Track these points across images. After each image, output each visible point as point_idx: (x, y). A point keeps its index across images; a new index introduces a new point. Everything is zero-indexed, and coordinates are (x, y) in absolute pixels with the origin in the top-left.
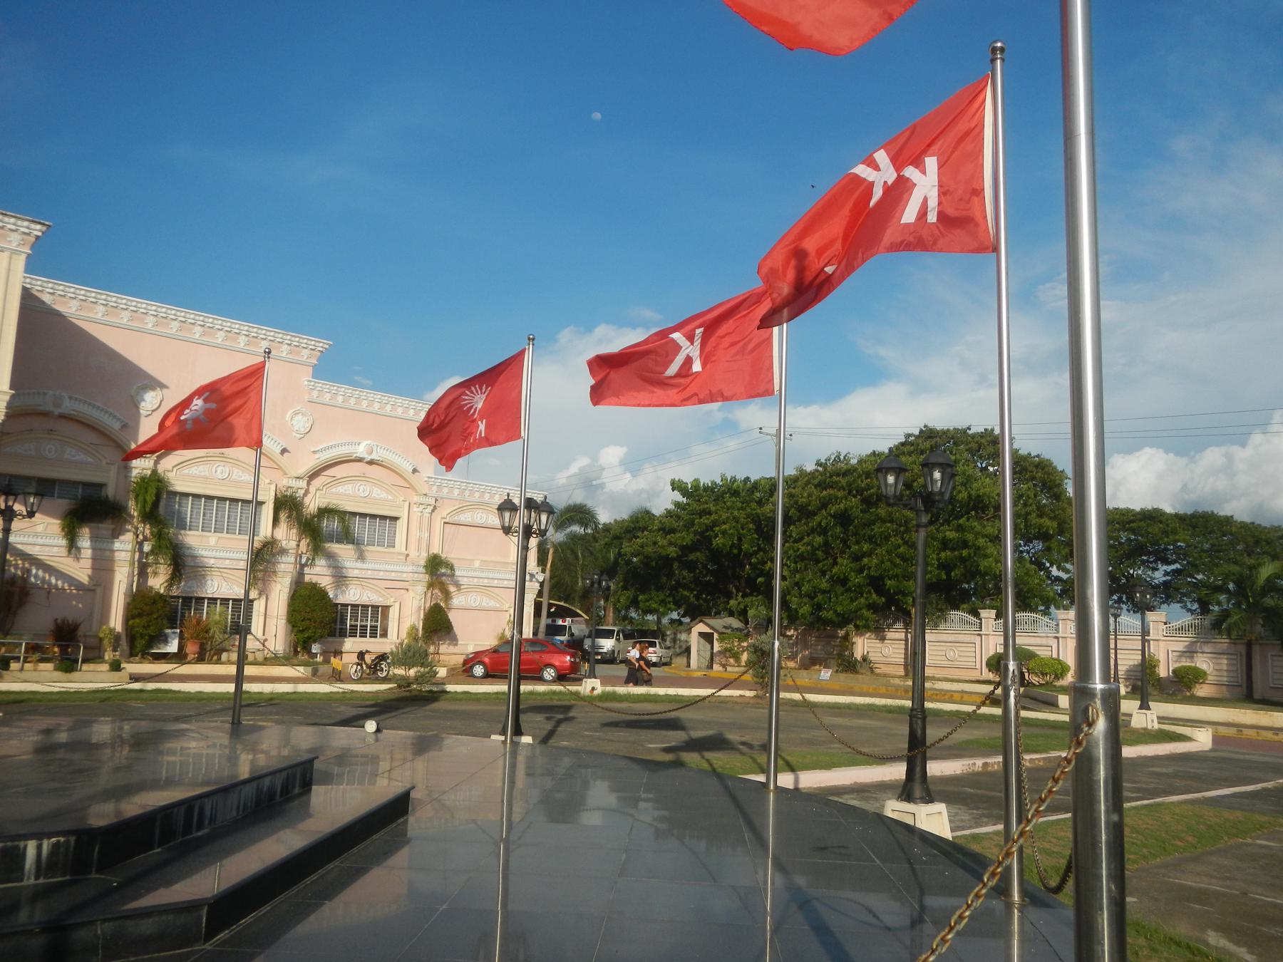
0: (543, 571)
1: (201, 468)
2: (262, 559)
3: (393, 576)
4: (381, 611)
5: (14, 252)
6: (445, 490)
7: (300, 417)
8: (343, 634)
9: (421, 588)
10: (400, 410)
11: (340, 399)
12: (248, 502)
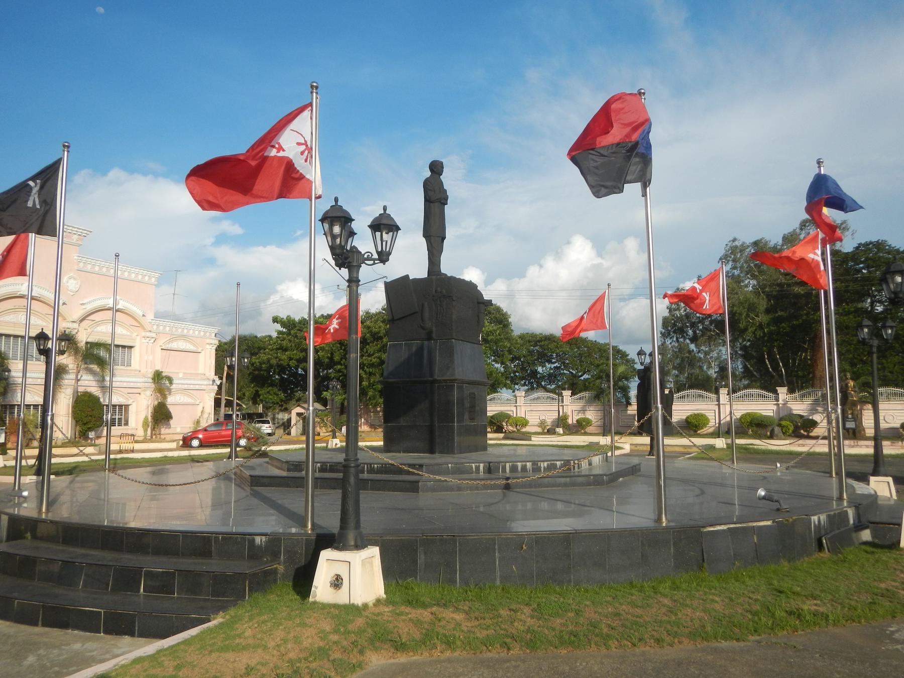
0: (221, 378)
1: (11, 316)
3: (132, 385)
4: (123, 408)
6: (161, 328)
7: (72, 281)
9: (149, 393)
10: (133, 276)
11: (97, 268)
12: (23, 337)
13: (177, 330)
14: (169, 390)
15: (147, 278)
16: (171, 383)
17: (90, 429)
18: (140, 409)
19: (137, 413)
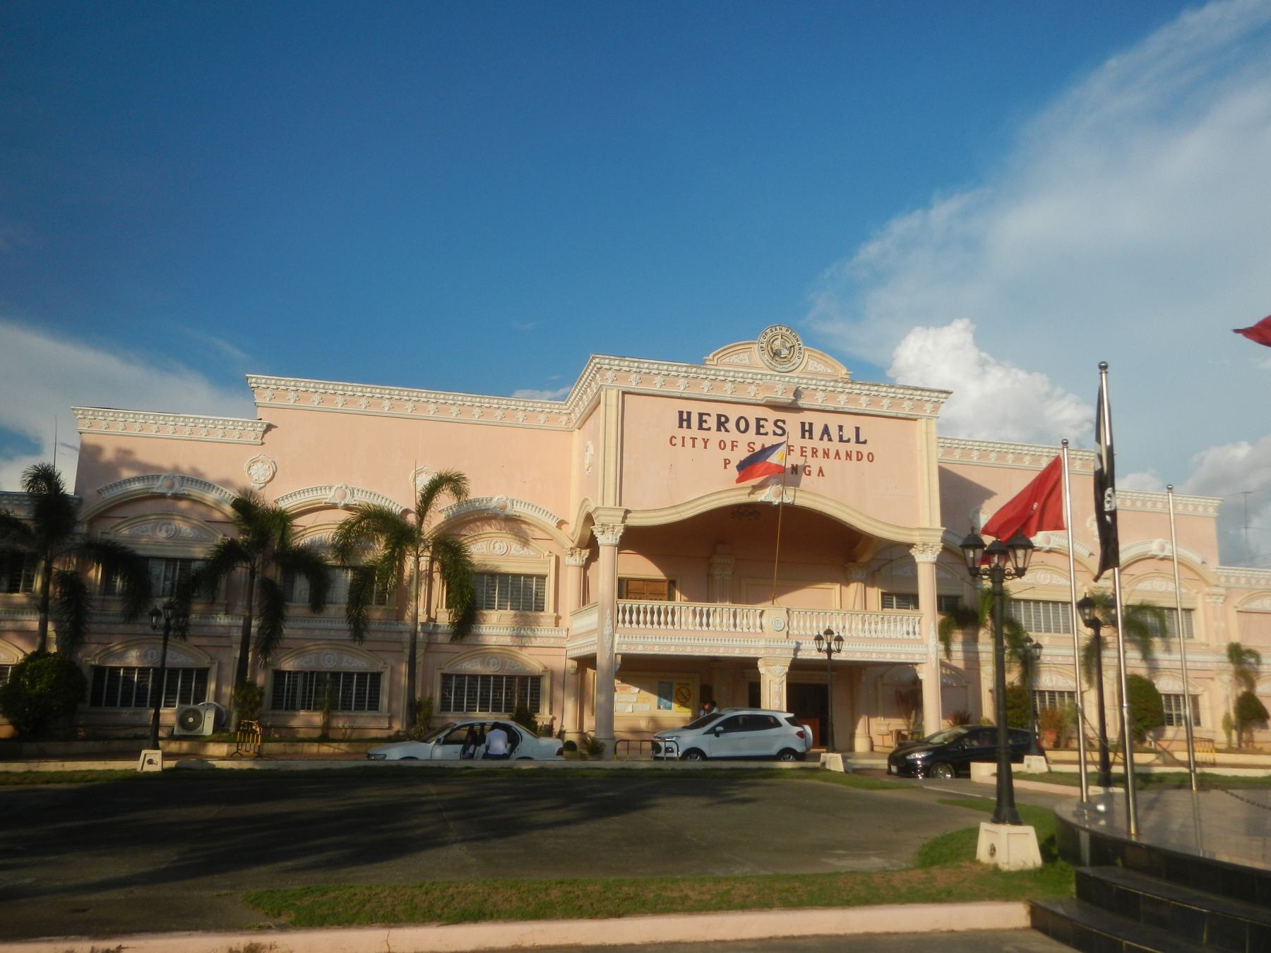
2: (1093, 655)
5: (929, 418)
6: (1233, 580)
8: (1163, 724)
13: (1258, 582)
14: (1258, 673)
15: (1201, 509)
16: (1259, 662)
17: (1148, 728)
18: (1217, 702)
19: (1212, 708)
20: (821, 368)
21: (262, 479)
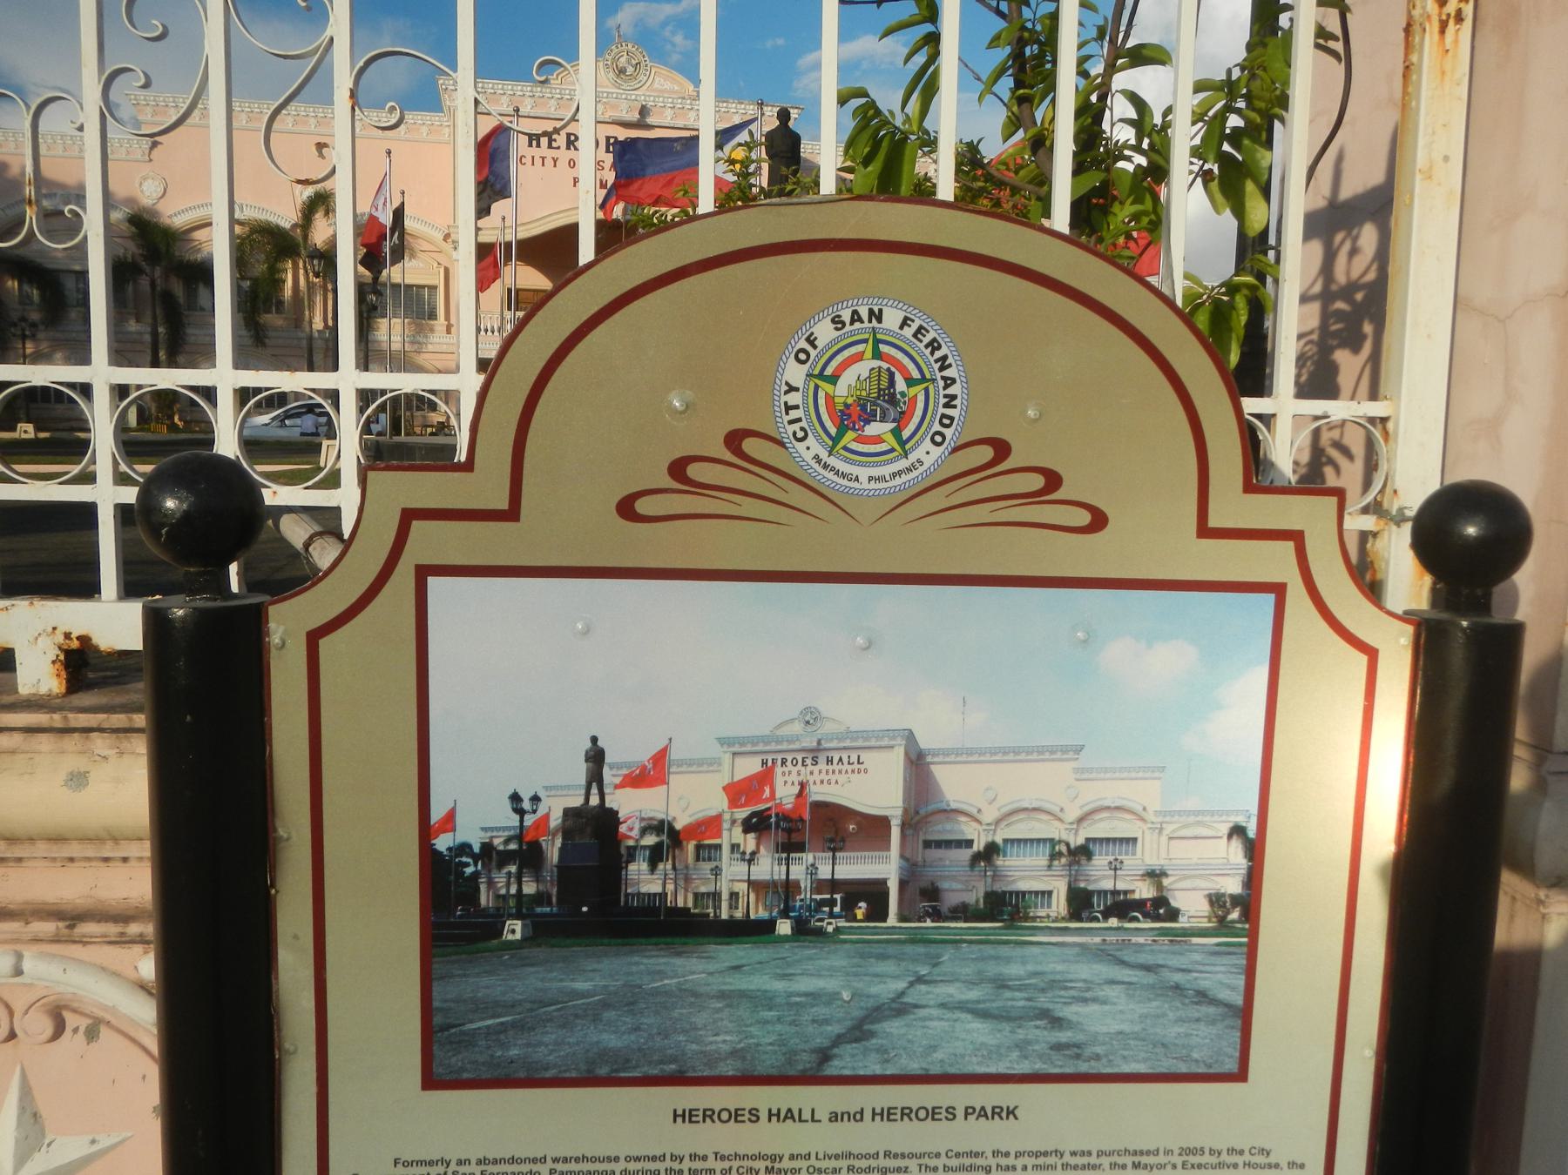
20: (668, 85)
21: (155, 195)
